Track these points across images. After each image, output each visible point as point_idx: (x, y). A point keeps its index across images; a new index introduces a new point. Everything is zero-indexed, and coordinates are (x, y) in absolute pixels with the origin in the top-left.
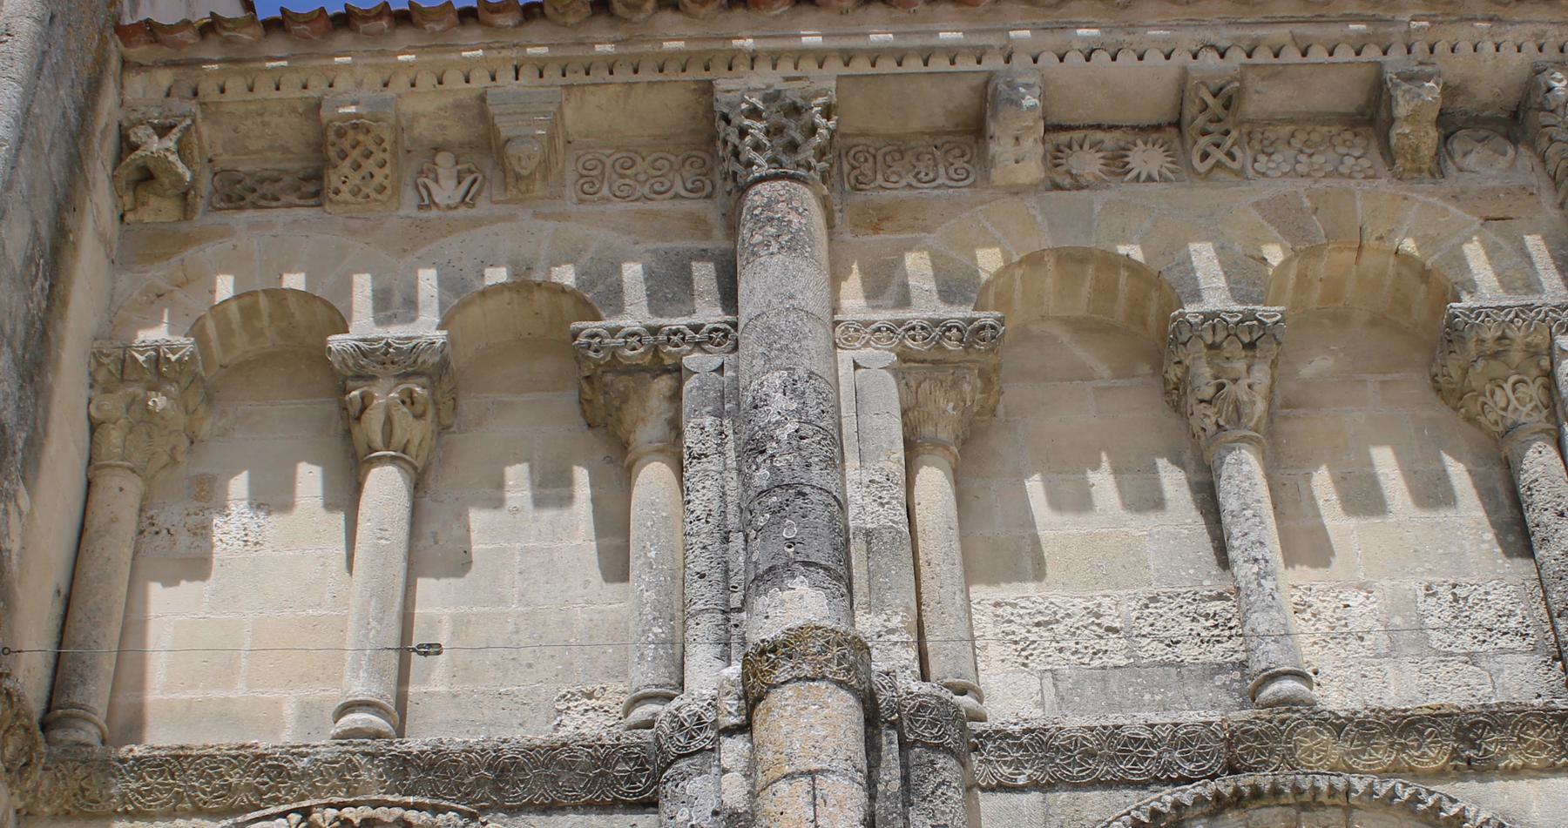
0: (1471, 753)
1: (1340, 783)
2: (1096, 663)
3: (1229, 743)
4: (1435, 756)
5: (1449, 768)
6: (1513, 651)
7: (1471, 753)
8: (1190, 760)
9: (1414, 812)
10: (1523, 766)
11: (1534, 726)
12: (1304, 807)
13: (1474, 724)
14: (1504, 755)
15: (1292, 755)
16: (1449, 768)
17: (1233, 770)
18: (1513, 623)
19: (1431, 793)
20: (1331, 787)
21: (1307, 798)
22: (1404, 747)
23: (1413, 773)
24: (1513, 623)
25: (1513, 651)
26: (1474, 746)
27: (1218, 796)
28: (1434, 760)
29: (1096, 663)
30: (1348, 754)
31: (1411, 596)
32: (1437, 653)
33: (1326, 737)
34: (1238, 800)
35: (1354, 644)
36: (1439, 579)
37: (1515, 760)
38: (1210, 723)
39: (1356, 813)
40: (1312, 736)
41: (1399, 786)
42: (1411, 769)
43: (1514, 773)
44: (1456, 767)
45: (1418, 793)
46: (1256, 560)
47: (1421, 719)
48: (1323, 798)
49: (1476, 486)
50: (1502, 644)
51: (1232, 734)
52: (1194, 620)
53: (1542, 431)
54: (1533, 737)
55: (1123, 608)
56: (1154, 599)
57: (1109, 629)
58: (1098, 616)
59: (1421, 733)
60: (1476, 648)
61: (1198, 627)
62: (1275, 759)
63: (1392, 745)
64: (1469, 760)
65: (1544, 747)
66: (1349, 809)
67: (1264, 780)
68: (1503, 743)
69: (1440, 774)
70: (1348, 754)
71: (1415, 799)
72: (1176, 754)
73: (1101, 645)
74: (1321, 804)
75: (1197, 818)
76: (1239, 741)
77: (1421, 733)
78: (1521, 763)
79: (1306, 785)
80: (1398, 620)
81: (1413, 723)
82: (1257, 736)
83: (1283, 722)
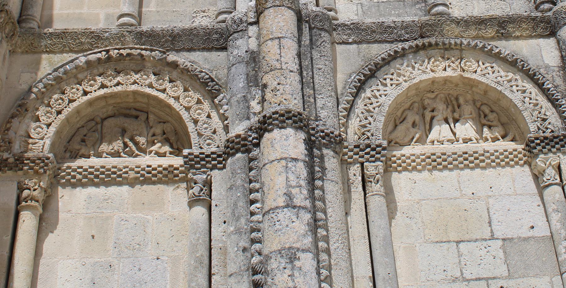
0: (503, 31)
1: (458, 41)
3: (421, 28)
4: (491, 32)
5: (495, 36)
7: (503, 31)
8: (407, 34)
9: (483, 51)
10: (521, 36)
11: (524, 22)
12: (446, 49)
13: (504, 21)
14: (514, 32)
15: (442, 32)
16: (495, 36)
17: (422, 37)
19: (489, 45)
20: (455, 43)
21: (447, 46)
22: (480, 29)
23: (483, 38)
26: (504, 29)
27: (417, 46)
30: (461, 31)
33: (454, 26)
37: (518, 34)
38: (414, 21)
39: (464, 51)
40: (449, 25)
42: (483, 37)
43: (517, 38)
44: (498, 36)
45: (485, 45)
47: (486, 20)
48: (453, 47)
54: (524, 25)
59: (486, 24)
62: (437, 33)
63: (476, 28)
64: (502, 34)
65: (527, 29)
66: (461, 50)
67: (433, 40)
68: (514, 28)
69: (493, 38)
70: (461, 31)
71: (484, 47)
72: (403, 32)
74: (452, 49)
75: (410, 53)
76: (424, 27)
77: (486, 24)
78: (520, 35)
79: (447, 42)
81: (483, 21)
82: (430, 25)
83: (439, 21)
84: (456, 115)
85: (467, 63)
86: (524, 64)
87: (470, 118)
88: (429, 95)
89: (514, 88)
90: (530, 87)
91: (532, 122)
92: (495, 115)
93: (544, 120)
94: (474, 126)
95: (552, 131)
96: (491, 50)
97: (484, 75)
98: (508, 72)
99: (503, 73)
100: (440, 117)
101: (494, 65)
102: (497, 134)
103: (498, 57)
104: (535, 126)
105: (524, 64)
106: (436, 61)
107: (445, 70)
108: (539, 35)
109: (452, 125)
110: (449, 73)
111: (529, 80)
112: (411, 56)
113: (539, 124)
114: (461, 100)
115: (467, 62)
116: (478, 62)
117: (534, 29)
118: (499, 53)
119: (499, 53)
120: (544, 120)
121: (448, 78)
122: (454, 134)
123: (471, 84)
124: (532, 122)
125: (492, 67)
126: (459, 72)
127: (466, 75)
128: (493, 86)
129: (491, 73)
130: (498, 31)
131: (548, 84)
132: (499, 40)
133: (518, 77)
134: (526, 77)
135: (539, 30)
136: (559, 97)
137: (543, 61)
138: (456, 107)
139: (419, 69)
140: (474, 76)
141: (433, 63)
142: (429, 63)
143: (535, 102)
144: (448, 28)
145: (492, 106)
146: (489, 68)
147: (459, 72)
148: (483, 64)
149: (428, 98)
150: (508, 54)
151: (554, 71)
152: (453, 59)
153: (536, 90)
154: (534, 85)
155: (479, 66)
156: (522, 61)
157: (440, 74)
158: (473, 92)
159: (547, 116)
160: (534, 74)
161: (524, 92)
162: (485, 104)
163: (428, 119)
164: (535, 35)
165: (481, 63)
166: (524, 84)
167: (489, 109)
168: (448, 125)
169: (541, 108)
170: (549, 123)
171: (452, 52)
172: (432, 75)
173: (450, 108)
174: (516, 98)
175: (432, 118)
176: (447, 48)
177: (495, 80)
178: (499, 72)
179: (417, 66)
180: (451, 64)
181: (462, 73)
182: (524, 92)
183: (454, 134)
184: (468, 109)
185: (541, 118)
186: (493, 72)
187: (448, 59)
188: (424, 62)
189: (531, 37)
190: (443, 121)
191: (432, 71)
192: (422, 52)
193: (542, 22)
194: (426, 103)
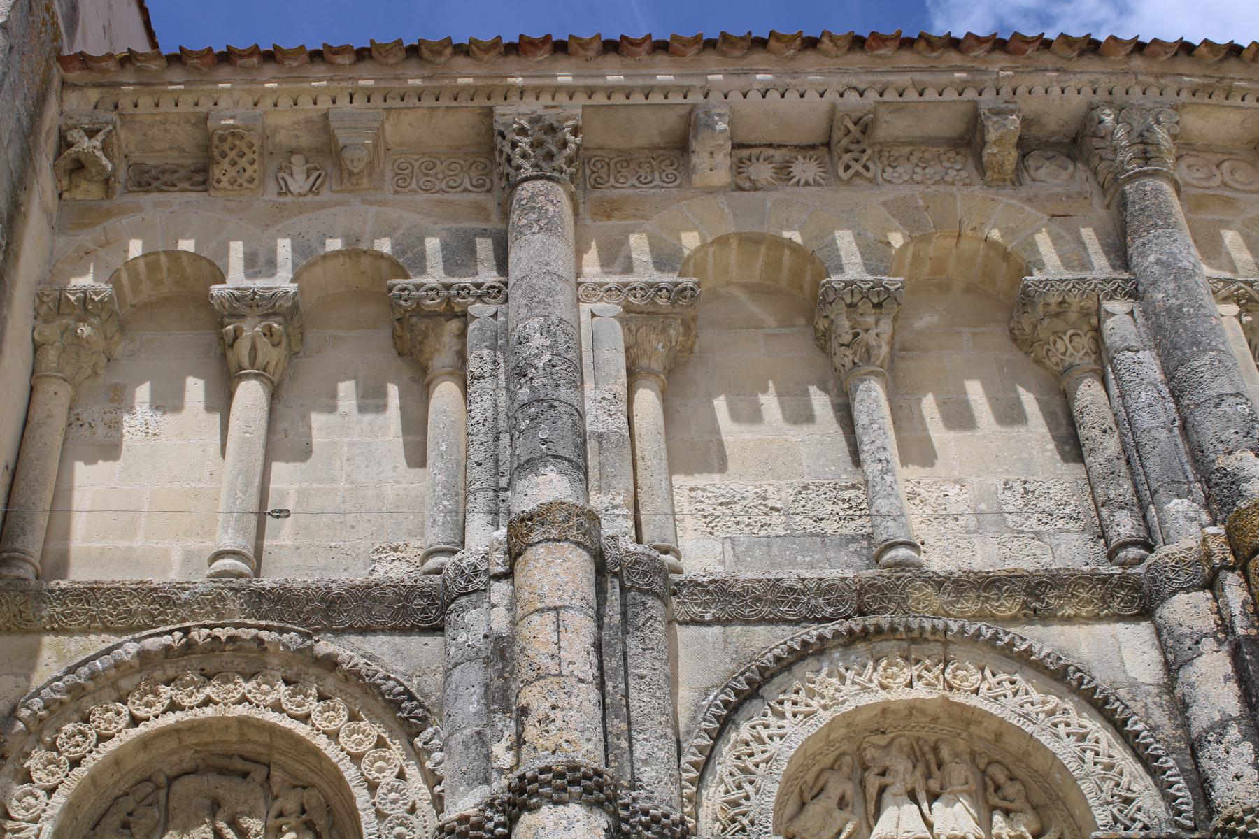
0: (1037, 605)
1: (940, 624)
2: (763, 533)
3: (859, 593)
4: (1010, 606)
5: (1020, 615)
6: (1068, 531)
7: (1037, 605)
8: (830, 605)
9: (994, 647)
10: (1076, 615)
11: (1083, 586)
12: (913, 641)
13: (1039, 584)
14: (1061, 607)
15: (905, 603)
16: (1020, 615)
18: (1068, 510)
19: (1007, 633)
20: (933, 627)
21: (916, 634)
22: (987, 599)
23: (994, 618)
24: (1068, 510)
25: (1068, 531)
26: (1038, 599)
27: (851, 632)
28: (1009, 609)
29: (763, 533)
30: (946, 603)
31: (993, 489)
32: (1012, 531)
34: (865, 635)
35: (951, 523)
36: (1013, 477)
37: (1069, 611)
39: (951, 646)
40: (920, 589)
41: (984, 628)
42: (992, 616)
43: (1068, 620)
44: (1025, 615)
45: (997, 633)
46: (880, 461)
47: (1000, 579)
48: (928, 635)
49: (1041, 409)
50: (1060, 525)
51: (862, 586)
52: (834, 503)
53: (1091, 371)
54: (1083, 594)
55: (783, 494)
56: (806, 488)
57: (773, 509)
58: (765, 499)
59: (1000, 589)
60: (1041, 528)
61: (837, 509)
62: (893, 606)
63: (978, 597)
64: (1035, 610)
65: (1090, 602)
66: (946, 643)
67: (884, 621)
68: (1060, 598)
69: (1014, 620)
70: (946, 603)
71: (995, 637)
72: (821, 601)
73: (767, 520)
74: (926, 640)
75: (835, 647)
76: (867, 592)
77: (1000, 589)
79: (915, 625)
80: (983, 507)
81: (994, 581)
82: (879, 589)
83: (898, 579)
84: (934, 785)
85: (959, 672)
86: (1082, 678)
87: (964, 791)
88: (875, 739)
89: (1062, 729)
90: (1095, 727)
91: (1101, 805)
92: (1018, 786)
93: (1127, 801)
94: (972, 811)
95: (1145, 827)
96: (1011, 644)
97: (996, 698)
98: (1047, 693)
99: (1036, 696)
100: (898, 787)
101: (1017, 677)
102: (1023, 829)
103: (1025, 660)
104: (1108, 813)
105: (1082, 678)
106: (890, 665)
107: (910, 685)
108: (1115, 614)
109: (925, 806)
110: (920, 692)
111: (1094, 712)
112: (837, 655)
113: (1115, 811)
114: (945, 753)
115: (957, 668)
116: (982, 670)
117: (1105, 602)
118: (1029, 651)
119: (1029, 651)
120: (1127, 801)
121: (917, 704)
122: (930, 826)
123: (967, 718)
124: (1101, 805)
125: (1013, 683)
126: (940, 691)
127: (956, 697)
128: (1015, 722)
129: (1009, 694)
130: (1025, 605)
131: (1136, 723)
132: (1027, 624)
133: (1069, 706)
134: (1088, 706)
135: (1116, 605)
136: (1160, 752)
137: (1125, 672)
138: (934, 767)
139: (854, 683)
140: (973, 701)
141: (885, 670)
142: (875, 669)
143: (1106, 760)
144: (917, 595)
145: (1012, 767)
146: (1007, 684)
147: (940, 691)
148: (994, 675)
149: (874, 746)
150: (1048, 655)
151: (1149, 694)
152: (928, 662)
153: (1110, 735)
154: (1106, 723)
155: (984, 678)
156: (1079, 670)
157: (900, 694)
158: (971, 735)
159: (1134, 792)
160: (1106, 701)
161: (1083, 737)
162: (997, 762)
163: (872, 790)
164: (1107, 615)
165: (988, 672)
166: (1084, 722)
167: (1006, 772)
168: (915, 807)
169: (1121, 774)
170: (1139, 809)
171: (925, 646)
172: (882, 696)
173: (921, 769)
174: (1065, 750)
175: (882, 790)
176: (916, 638)
177: (1019, 710)
178: (1027, 693)
179: (849, 675)
180: (924, 673)
181: (948, 694)
182: (1083, 737)
183: (930, 826)
184: (959, 772)
185: (1120, 796)
186: (1015, 694)
187: (917, 662)
188: (865, 666)
189: (1097, 619)
190: (906, 798)
191: (883, 687)
192: (861, 647)
193: (1122, 587)
194: (868, 757)
